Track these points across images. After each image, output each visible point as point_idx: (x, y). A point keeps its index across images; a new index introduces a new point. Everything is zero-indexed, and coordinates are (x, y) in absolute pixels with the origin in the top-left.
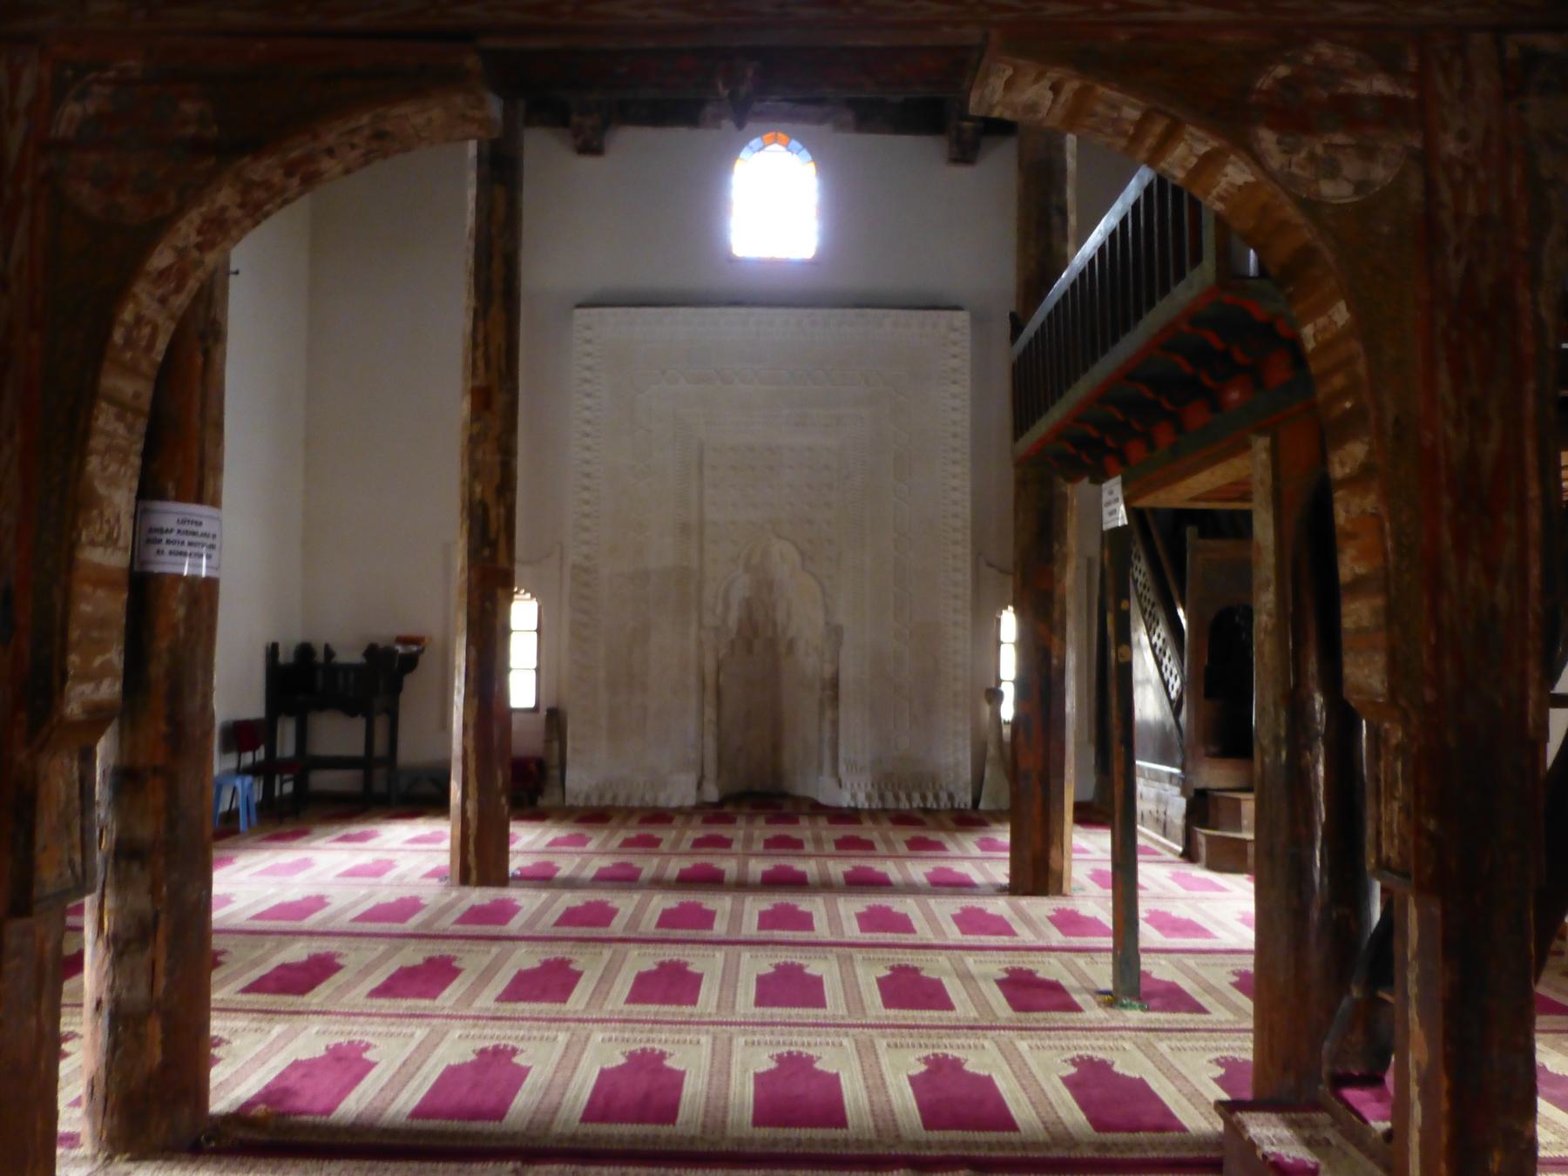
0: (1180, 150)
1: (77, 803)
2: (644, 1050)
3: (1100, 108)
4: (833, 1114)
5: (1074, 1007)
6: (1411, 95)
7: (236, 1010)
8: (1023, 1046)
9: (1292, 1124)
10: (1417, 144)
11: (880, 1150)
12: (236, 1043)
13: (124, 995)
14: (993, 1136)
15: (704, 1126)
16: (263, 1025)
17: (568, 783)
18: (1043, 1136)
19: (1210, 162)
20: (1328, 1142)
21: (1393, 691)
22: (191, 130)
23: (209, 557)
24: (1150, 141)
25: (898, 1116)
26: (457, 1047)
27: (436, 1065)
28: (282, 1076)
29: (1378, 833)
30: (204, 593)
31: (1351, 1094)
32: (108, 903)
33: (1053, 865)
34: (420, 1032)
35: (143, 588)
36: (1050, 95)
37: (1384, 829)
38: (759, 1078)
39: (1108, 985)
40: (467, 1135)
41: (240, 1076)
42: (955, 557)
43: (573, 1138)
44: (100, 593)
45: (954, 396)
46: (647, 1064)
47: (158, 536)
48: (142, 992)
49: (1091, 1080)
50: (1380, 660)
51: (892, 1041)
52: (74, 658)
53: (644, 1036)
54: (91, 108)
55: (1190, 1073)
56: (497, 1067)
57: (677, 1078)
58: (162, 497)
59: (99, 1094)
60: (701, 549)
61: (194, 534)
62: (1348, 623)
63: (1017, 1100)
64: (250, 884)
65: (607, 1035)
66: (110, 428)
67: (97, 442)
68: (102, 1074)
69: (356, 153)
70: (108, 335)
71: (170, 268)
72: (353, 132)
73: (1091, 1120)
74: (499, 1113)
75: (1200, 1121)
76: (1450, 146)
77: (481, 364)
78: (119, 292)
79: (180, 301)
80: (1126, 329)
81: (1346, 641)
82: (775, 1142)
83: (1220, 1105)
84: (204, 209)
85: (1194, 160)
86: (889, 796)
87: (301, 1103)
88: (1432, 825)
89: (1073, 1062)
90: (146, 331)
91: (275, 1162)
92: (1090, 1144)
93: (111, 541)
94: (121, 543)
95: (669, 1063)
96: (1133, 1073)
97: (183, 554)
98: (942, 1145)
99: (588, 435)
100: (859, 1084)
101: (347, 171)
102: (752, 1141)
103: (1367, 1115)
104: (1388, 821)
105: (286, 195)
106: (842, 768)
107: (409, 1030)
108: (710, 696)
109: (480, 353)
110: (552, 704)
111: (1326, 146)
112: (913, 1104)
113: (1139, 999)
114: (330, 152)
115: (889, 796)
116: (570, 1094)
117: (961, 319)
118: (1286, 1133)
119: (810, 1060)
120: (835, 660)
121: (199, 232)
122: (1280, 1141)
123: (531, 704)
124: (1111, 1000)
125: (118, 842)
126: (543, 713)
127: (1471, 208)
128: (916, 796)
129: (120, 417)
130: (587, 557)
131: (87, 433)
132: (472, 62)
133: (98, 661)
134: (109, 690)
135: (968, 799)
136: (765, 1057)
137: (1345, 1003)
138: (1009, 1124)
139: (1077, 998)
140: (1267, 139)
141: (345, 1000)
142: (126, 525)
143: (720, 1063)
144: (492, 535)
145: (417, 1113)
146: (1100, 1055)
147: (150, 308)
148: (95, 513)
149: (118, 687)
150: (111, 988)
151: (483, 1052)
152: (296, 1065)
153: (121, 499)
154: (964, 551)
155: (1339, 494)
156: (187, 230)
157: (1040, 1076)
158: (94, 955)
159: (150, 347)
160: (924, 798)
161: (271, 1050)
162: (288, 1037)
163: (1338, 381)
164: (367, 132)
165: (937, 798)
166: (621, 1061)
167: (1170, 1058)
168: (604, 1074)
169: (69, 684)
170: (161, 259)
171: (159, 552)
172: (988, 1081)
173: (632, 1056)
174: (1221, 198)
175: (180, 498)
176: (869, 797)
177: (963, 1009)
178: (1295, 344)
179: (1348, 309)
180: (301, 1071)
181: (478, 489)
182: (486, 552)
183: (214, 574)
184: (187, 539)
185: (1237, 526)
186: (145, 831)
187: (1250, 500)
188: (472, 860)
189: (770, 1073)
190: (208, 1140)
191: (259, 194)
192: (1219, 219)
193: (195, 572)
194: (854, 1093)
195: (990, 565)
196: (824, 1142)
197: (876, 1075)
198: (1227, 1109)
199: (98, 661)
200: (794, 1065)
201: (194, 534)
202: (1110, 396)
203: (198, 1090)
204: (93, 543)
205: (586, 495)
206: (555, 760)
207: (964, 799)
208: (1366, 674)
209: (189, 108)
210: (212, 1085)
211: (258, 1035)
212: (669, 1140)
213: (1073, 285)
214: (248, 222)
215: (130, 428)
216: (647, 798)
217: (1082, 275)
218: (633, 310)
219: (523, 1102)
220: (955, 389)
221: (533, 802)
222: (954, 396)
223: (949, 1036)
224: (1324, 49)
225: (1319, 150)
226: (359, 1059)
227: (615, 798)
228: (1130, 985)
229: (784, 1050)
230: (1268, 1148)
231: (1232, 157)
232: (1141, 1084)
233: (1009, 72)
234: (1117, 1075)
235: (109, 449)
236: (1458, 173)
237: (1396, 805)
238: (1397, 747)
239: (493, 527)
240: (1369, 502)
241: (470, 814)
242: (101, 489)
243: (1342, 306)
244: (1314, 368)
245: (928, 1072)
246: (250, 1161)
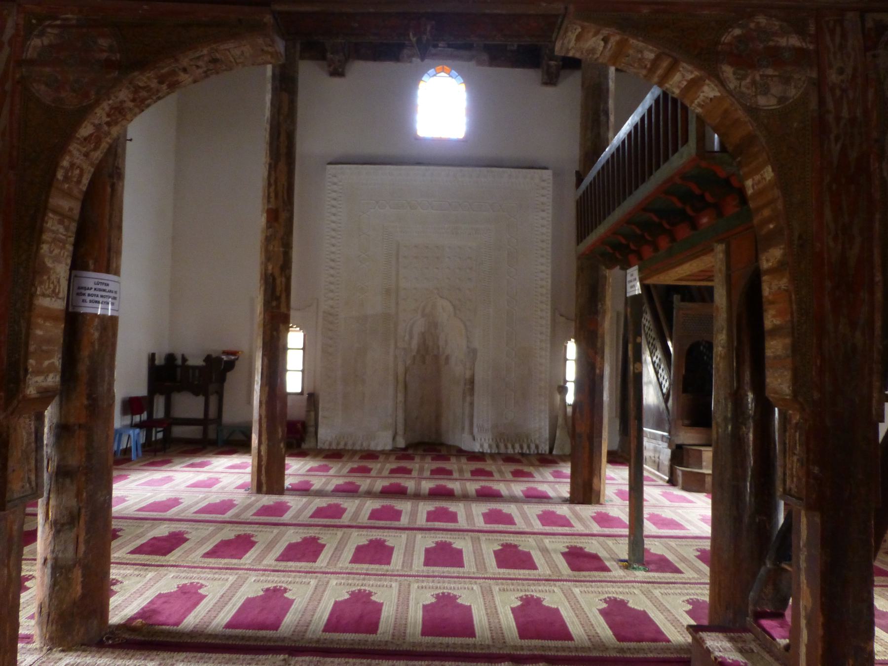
0: (677, 77)
1: (33, 445)
2: (360, 590)
3: (631, 52)
4: (467, 629)
5: (606, 569)
6: (811, 47)
7: (127, 564)
8: (577, 591)
9: (731, 640)
10: (814, 75)
11: (494, 651)
12: (126, 583)
13: (60, 555)
14: (559, 643)
15: (393, 635)
16: (142, 573)
17: (319, 436)
18: (587, 644)
19: (694, 85)
20: (752, 651)
21: (795, 393)
22: (105, 55)
23: (113, 304)
24: (660, 72)
25: (504, 631)
26: (253, 587)
27: (240, 598)
28: (152, 602)
29: (785, 474)
30: (109, 325)
31: (766, 623)
32: (52, 502)
33: (595, 487)
34: (232, 578)
35: (73, 321)
36: (602, 44)
37: (788, 472)
38: (425, 607)
39: (626, 557)
40: (256, 639)
41: (128, 602)
42: (542, 310)
43: (318, 641)
44: (48, 324)
45: (543, 218)
46: (361, 598)
47: (83, 291)
48: (70, 554)
49: (616, 612)
50: (788, 375)
51: (502, 587)
52: (32, 362)
53: (360, 582)
54: (46, 41)
55: (673, 608)
56: (275, 598)
57: (378, 607)
58: (86, 268)
59: (45, 610)
60: (397, 304)
61: (104, 290)
62: (769, 353)
63: (573, 623)
64: (135, 491)
65: (339, 581)
66: (54, 228)
67: (46, 237)
68: (47, 600)
69: (200, 71)
70: (54, 175)
71: (91, 135)
72: (198, 58)
73: (615, 634)
74: (276, 626)
75: (678, 636)
76: (833, 77)
77: (272, 195)
78: (61, 149)
79: (97, 155)
80: (643, 181)
81: (768, 363)
82: (434, 645)
83: (690, 627)
84: (111, 102)
85: (685, 83)
86: (502, 446)
87: (162, 618)
88: (816, 470)
89: (605, 601)
90: (77, 172)
91: (146, 653)
92: (615, 648)
93: (55, 294)
94: (61, 295)
95: (373, 598)
96: (640, 608)
97: (98, 302)
98: (529, 648)
99: (333, 237)
100: (483, 612)
101: (195, 82)
102: (420, 644)
103: (775, 635)
104: (789, 468)
105: (160, 94)
106: (475, 430)
107: (226, 577)
108: (401, 387)
109: (272, 189)
110: (311, 391)
111: (761, 76)
112: (513, 624)
113: (643, 565)
114: (185, 70)
115: (502, 446)
116: (317, 616)
117: (547, 174)
118: (728, 645)
119: (455, 598)
120: (472, 368)
121: (108, 115)
122: (725, 649)
123: (299, 390)
124: (627, 565)
125: (58, 467)
126: (306, 396)
127: (845, 113)
128: (517, 446)
129: (61, 222)
130: (332, 307)
131: (41, 231)
132: (268, 18)
133: (46, 363)
134: (53, 380)
135: (547, 448)
136: (429, 595)
137: (763, 571)
138: (568, 636)
139: (608, 564)
140: (728, 71)
141: (189, 559)
142: (64, 284)
143: (403, 599)
144: (278, 294)
145: (228, 626)
146: (621, 597)
147: (79, 159)
148: (45, 277)
149: (58, 379)
150: (53, 552)
151: (268, 590)
152: (160, 596)
153: (61, 270)
154: (547, 307)
155: (765, 278)
156: (100, 114)
157: (586, 609)
158: (43, 532)
159: (79, 182)
160: (521, 447)
161: (146, 587)
162: (156, 580)
163: (766, 213)
164: (206, 59)
165: (529, 447)
166: (347, 596)
167: (660, 598)
168: (336, 603)
169: (29, 376)
170: (86, 130)
171: (84, 301)
172: (557, 611)
173: (353, 594)
174: (699, 105)
175: (95, 271)
176: (490, 446)
177: (543, 569)
178: (741, 191)
179: (773, 170)
180: (163, 600)
181: (270, 267)
182: (274, 304)
183: (115, 314)
184: (100, 293)
185: (705, 295)
186: (73, 461)
187: (712, 281)
189: (432, 604)
190: (108, 639)
191: (144, 94)
192: (699, 118)
193: (104, 312)
194: (480, 618)
195: (561, 315)
196: (462, 646)
197: (493, 607)
198: (694, 630)
199: (46, 363)
200: (446, 600)
201: (104, 290)
202: (632, 219)
203: (103, 610)
204: (44, 295)
205: (332, 272)
206: (312, 423)
207: (545, 448)
208: (779, 382)
209: (103, 42)
210: (111, 607)
211: (138, 578)
212: (373, 643)
213: (613, 155)
214: (137, 110)
215: (67, 229)
216: (364, 445)
217: (618, 149)
218: (360, 166)
219: (290, 620)
220: (544, 214)
221: (299, 446)
222: (543, 218)
223: (534, 585)
224: (762, 20)
225: (758, 78)
226: (196, 593)
227: (346, 444)
228: (638, 556)
229: (440, 591)
230: (717, 654)
231: (707, 81)
232: (644, 613)
233: (579, 30)
234: (630, 609)
235: (55, 240)
236: (838, 92)
237: (795, 458)
238: (797, 424)
239: (278, 289)
240: (784, 283)
241: (263, 453)
242: (49, 264)
243: (769, 169)
244: (752, 205)
245: (522, 605)
246: (131, 652)
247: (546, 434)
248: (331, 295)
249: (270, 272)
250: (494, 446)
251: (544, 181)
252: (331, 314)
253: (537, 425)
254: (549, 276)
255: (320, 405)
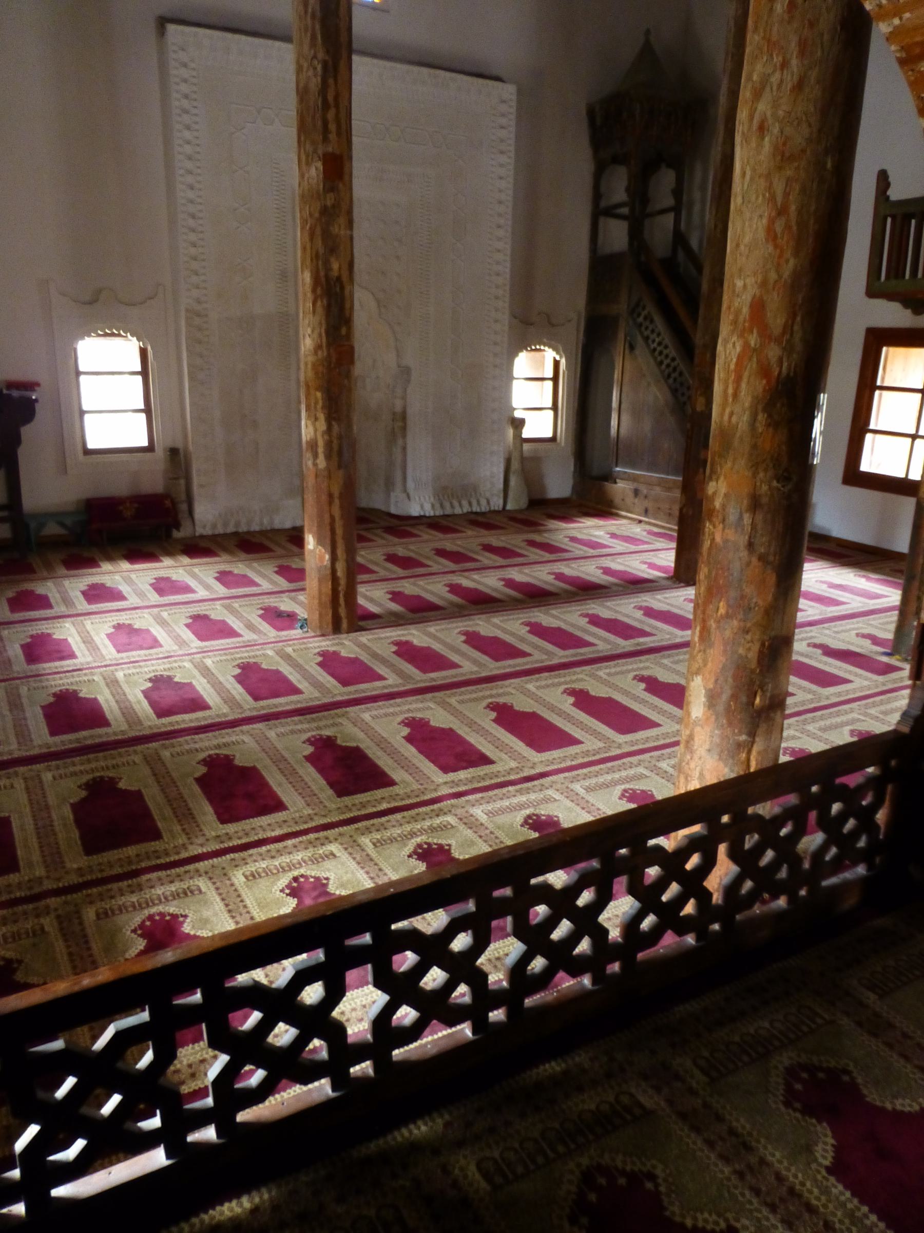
42: (497, 310)
45: (501, 165)
86: (447, 505)
106: (410, 484)
109: (331, 115)
115: (447, 505)
123: (145, 443)
126: (160, 452)
135: (501, 502)
160: (470, 504)
165: (478, 503)
176: (433, 506)
181: (335, 266)
188: (342, 611)
206: (183, 497)
216: (265, 521)
220: (503, 159)
221: (169, 536)
222: (501, 165)
227: (237, 524)
241: (340, 574)
247: (501, 486)
248: (194, 279)
249: (335, 273)
250: (438, 506)
251: (503, 102)
252: (199, 315)
253: (488, 473)
254: (508, 258)
255: (195, 466)
